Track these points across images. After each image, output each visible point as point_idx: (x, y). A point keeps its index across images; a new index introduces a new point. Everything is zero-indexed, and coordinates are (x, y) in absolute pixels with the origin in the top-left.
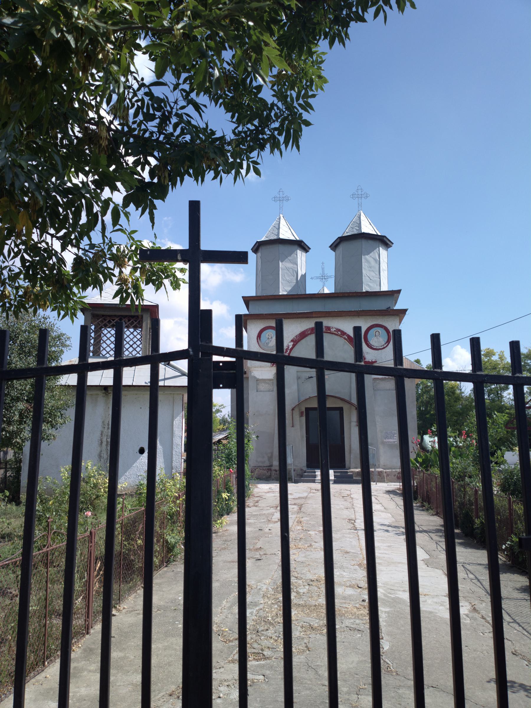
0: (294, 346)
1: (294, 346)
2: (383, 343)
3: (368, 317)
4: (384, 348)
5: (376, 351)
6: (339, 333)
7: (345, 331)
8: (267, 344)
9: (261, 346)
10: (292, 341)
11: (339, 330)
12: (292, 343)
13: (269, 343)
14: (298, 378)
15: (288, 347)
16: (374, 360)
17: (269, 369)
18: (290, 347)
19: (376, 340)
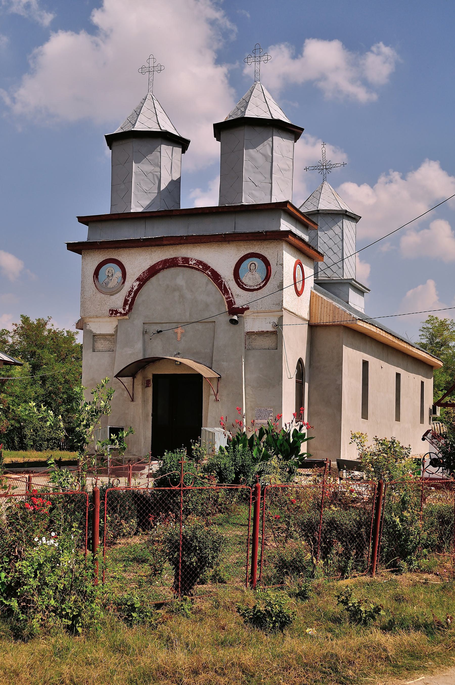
0: (140, 287)
1: (140, 287)
2: (260, 281)
3: (241, 243)
4: (260, 288)
5: (250, 293)
6: (201, 267)
7: (209, 265)
8: (107, 284)
9: (98, 287)
10: (138, 279)
11: (200, 263)
12: (138, 283)
13: (108, 283)
14: (145, 332)
15: (133, 288)
16: (245, 307)
17: (108, 319)
18: (135, 288)
19: (251, 276)
